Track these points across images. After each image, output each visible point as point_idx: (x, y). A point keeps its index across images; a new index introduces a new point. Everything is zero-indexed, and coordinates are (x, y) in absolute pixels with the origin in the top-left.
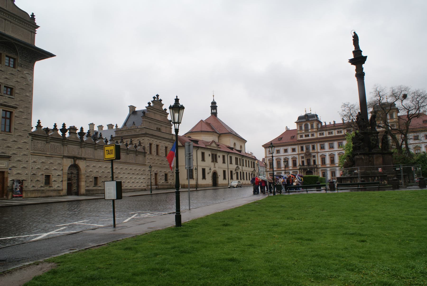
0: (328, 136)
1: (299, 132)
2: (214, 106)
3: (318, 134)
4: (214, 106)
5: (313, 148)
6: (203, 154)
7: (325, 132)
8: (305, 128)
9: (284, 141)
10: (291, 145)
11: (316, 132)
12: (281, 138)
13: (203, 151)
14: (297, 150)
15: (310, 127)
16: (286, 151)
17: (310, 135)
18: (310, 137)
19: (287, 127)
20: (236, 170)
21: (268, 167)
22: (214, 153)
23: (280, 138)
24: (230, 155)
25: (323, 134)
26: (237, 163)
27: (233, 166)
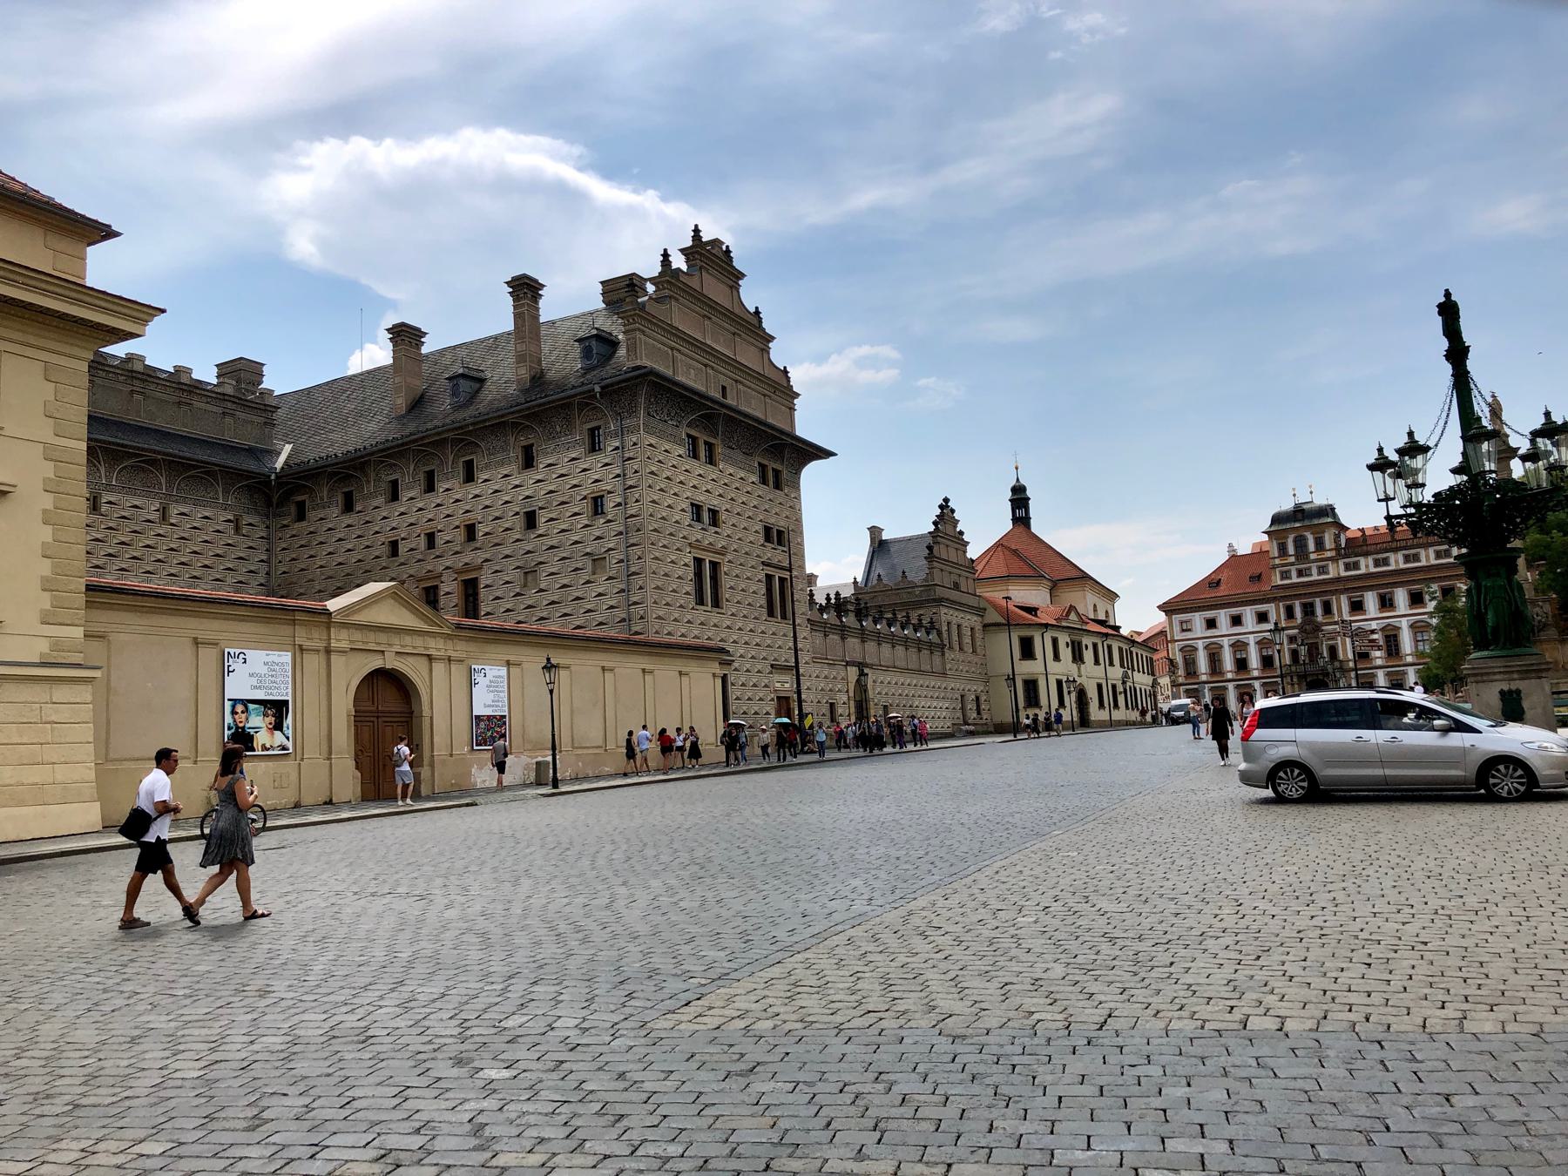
0: (1373, 570)
1: (1277, 561)
2: (1019, 499)
3: (1342, 567)
4: (1019, 499)
5: (1327, 609)
6: (1055, 641)
7: (1362, 561)
8: (1296, 547)
9: (1223, 590)
10: (1254, 602)
11: (1333, 560)
12: (1218, 583)
13: (1055, 634)
14: (1273, 617)
15: (1311, 546)
16: (1237, 621)
17: (1314, 571)
18: (1315, 577)
19: (1230, 545)
20: (1124, 683)
21: (1181, 672)
22: (1077, 638)
23: (1212, 582)
24: (1109, 642)
25: (1356, 566)
26: (1122, 666)
27: (1116, 673)
